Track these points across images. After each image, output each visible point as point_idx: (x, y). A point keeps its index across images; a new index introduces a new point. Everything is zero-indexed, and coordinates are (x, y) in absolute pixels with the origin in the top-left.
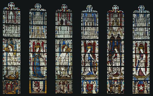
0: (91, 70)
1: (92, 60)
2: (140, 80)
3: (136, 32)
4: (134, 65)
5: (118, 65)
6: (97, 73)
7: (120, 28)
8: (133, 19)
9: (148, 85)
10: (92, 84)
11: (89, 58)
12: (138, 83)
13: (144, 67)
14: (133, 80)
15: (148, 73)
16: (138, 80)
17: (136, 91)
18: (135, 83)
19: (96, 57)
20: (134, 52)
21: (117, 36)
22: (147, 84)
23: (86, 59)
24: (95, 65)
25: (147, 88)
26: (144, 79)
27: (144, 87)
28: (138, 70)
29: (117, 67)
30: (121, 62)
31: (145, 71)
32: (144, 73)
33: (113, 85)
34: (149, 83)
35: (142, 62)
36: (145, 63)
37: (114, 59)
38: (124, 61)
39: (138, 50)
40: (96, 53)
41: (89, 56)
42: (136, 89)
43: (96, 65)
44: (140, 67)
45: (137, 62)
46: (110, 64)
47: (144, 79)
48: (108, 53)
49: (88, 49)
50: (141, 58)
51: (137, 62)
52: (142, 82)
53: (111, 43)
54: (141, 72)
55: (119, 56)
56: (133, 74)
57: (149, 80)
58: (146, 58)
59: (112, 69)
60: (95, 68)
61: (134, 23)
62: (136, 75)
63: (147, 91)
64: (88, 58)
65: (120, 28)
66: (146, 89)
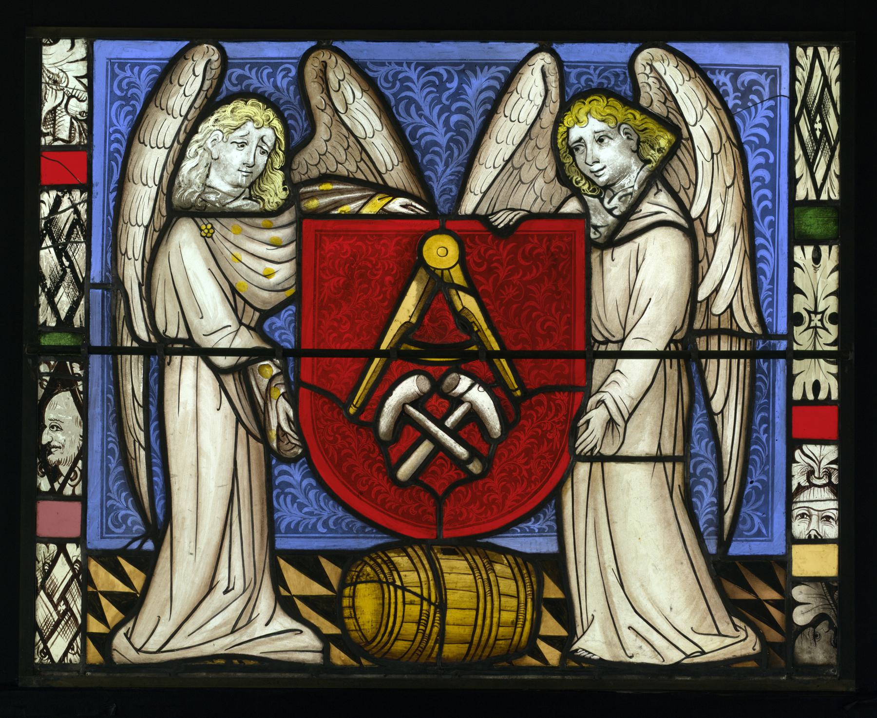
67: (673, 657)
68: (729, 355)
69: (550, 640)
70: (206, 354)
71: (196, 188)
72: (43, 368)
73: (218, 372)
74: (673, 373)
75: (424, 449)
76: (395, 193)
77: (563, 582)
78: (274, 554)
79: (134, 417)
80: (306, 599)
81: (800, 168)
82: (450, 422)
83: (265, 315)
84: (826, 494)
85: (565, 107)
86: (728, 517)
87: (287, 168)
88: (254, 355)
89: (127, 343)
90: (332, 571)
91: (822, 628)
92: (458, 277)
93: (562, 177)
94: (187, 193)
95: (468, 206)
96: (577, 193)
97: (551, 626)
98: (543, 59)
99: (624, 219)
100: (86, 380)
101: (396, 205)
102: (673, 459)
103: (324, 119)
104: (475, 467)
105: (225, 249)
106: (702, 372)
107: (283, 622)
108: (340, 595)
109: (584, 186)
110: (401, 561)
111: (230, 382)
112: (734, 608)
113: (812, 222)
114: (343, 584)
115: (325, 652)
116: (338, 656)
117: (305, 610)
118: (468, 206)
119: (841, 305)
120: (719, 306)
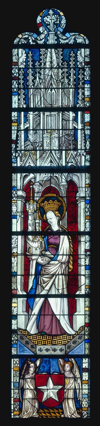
2: (45, 353)
4: (18, 285)
9: (81, 377)
12: (36, 367)
13: (61, 296)
14: (14, 352)
15: (80, 320)
16: (38, 353)
18: (21, 370)
20: (17, 226)
22: (77, 374)
26: (61, 350)
27: (63, 388)
28: (36, 310)
31: (66, 312)
32: (64, 322)
34: (85, 370)
35: (54, 268)
39: (38, 215)
42: (29, 395)
44: (44, 292)
45: (33, 271)
47: (61, 350)
50: (48, 253)
51: (33, 271)
52: (53, 362)
54: (48, 319)
56: (14, 327)
57: (85, 356)
58: (74, 255)
62: (24, 333)
63: (79, 407)
66: (71, 394)
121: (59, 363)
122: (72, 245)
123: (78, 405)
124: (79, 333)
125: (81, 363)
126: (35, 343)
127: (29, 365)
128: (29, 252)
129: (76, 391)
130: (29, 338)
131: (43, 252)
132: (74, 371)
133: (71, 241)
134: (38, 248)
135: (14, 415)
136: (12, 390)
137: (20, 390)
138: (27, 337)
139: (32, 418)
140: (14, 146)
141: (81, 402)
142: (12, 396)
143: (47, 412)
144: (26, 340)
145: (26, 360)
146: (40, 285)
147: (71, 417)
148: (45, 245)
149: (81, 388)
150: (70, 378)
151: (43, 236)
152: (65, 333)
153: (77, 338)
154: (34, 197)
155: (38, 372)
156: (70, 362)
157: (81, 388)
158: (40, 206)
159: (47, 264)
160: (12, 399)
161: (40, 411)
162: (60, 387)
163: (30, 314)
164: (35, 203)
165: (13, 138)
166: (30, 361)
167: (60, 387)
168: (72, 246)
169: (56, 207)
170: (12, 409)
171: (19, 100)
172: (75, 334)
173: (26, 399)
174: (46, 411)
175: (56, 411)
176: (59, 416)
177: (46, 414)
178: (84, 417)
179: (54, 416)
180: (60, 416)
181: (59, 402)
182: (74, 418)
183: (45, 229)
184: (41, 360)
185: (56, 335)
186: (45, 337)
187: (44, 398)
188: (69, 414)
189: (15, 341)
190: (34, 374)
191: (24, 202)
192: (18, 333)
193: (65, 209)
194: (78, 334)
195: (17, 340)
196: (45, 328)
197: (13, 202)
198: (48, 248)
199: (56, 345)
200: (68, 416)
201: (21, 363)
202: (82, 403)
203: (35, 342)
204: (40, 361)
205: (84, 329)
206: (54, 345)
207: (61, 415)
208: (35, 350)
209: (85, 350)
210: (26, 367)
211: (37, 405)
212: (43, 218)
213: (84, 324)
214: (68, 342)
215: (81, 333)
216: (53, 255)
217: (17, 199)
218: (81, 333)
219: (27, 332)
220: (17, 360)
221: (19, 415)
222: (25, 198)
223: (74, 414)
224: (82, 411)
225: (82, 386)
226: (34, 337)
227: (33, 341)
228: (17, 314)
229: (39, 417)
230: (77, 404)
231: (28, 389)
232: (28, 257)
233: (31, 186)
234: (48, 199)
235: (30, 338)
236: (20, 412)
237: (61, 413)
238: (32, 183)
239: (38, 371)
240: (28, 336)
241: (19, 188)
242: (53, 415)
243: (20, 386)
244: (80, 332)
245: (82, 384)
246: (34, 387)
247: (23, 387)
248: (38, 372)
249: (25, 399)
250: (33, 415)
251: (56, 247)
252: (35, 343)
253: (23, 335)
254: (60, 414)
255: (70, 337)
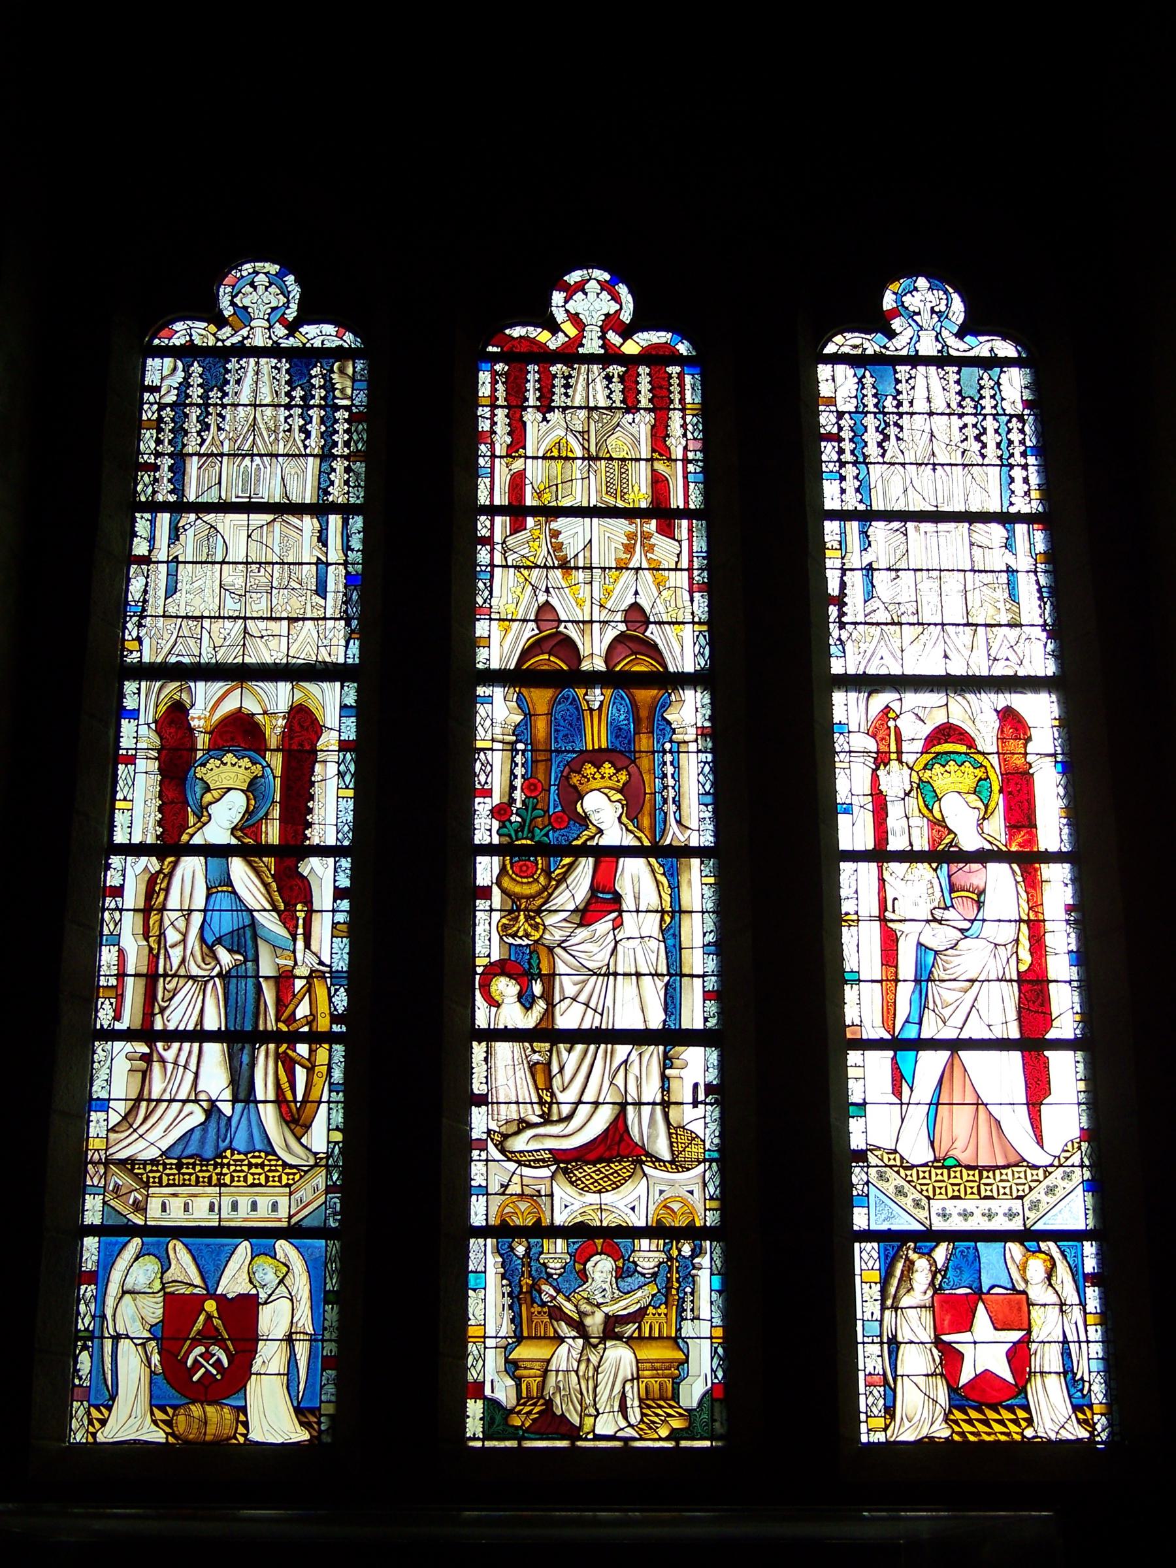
0: (234, 1082)
1: (264, 951)
2: (957, 1224)
3: (869, 569)
5: (627, 1019)
6: (319, 1137)
7: (646, 536)
8: (827, 421)
9: (1083, 1304)
10: (243, 1287)
11: (225, 923)
16: (939, 1225)
17: (910, 1398)
19: (323, 897)
21: (611, 634)
22: (1070, 1293)
23: (172, 936)
24: (303, 1010)
25: (1066, 1354)
27: (1026, 1341)
29: (622, 1051)
30: (675, 976)
33: (557, 1314)
36: (1022, 980)
37: (583, 933)
38: (712, 964)
40: (322, 851)
41: (221, 884)
43: (312, 1019)
45: (907, 967)
46: (526, 1000)
47: (1011, 1215)
48: (489, 850)
49: (208, 789)
51: (907, 967)
53: (529, 715)
55: (650, 898)
56: (857, 1142)
59: (542, 1075)
60: (289, 1065)
61: (842, 464)
64: (197, 918)
65: (646, 536)
67: (280, 1441)
68: (303, 1340)
69: (241, 1435)
70: (132, 1339)
71: (132, 1284)
72: (79, 1343)
73: (136, 1345)
74: (284, 1346)
75: (203, 1370)
76: (196, 1286)
77: (246, 1415)
78: (151, 1406)
79: (108, 1360)
80: (162, 1421)
81: (328, 1280)
82: (211, 1362)
83: (152, 1326)
84: (333, 1386)
85: (252, 1259)
86: (301, 1394)
87: (161, 1278)
88: (149, 1339)
89: (107, 1335)
90: (170, 1411)
91: (330, 1431)
92: (216, 1315)
93: (251, 1282)
94: (128, 1287)
95: (219, 1292)
96: (255, 1287)
97: (241, 1429)
98: (246, 1243)
99: (270, 1296)
100: (92, 1347)
101: (196, 1291)
102: (284, 1374)
103: (173, 1262)
104: (219, 1377)
105: (140, 1305)
106: (294, 1346)
107: (154, 1428)
108: (172, 1419)
109: (257, 1284)
110: (193, 1408)
111: (139, 1348)
112: (302, 1424)
113: (331, 1297)
114: (174, 1415)
115: (167, 1438)
116: (171, 1440)
117: (160, 1424)
118: (219, 1292)
119: (339, 1324)
120: (300, 1324)
121: (1008, 1256)
122: (1026, 891)
123: (1079, 1394)
124: (1062, 1160)
125: (1080, 1257)
126: (925, 1193)
127: (913, 1263)
128: (894, 911)
129: (1069, 1348)
130: (906, 1176)
131: (938, 914)
132: (1059, 1281)
133: (1020, 879)
134: (921, 902)
135: (869, 1430)
136: (860, 1347)
137: (886, 1346)
138: (898, 1173)
139: (927, 1445)
140: (833, 611)
141: (1087, 1385)
142: (861, 1366)
143: (978, 1420)
144: (896, 1183)
145: (900, 1248)
146: (934, 1011)
147: (1059, 1436)
148: (942, 891)
149: (1083, 1338)
150: (1045, 1305)
151: (934, 865)
152: (1021, 1161)
153: (1059, 1178)
154: (899, 752)
155: (941, 1288)
156: (1044, 1253)
157: (1083, 1338)
158: (920, 779)
159: (952, 948)
160: (861, 1375)
161: (952, 1417)
162: (1016, 1335)
163: (905, 1099)
164: (906, 771)
165: (830, 591)
166: (915, 1251)
167: (1016, 1335)
168: (1024, 895)
169: (969, 782)
170: (863, 1408)
171: (843, 491)
172: (1051, 1165)
173: (908, 1376)
174: (974, 1414)
175: (1007, 1415)
176: (1017, 1433)
177: (974, 1426)
178: (1099, 1435)
179: (1002, 1433)
180: (1022, 1434)
181: (1016, 1385)
182: (1068, 1441)
183: (940, 844)
184: (951, 1246)
185: (994, 1168)
186: (955, 1172)
187: (966, 1376)
188: (1049, 1425)
189: (860, 1187)
190: (930, 1293)
191: (874, 767)
192: (870, 1160)
193: (996, 787)
194: (1061, 1165)
195: (867, 1183)
196: (954, 1146)
197: (837, 765)
198: (952, 899)
199: (992, 1198)
200: (1048, 1431)
201: (886, 1257)
202: (1090, 1390)
203: (925, 1188)
204: (947, 1249)
205: (1079, 1148)
206: (986, 1198)
207: (1023, 1430)
208: (927, 1215)
209: (1086, 1214)
210: (902, 1271)
211: (942, 1395)
212: (931, 811)
213: (1077, 1134)
214: (1031, 1189)
215: (1069, 1162)
216: (969, 920)
217: (852, 759)
218: (1069, 1162)
219: (897, 1156)
220: (871, 1247)
221: (885, 1429)
222: (875, 755)
223: (1066, 1426)
224: (1093, 1414)
225: (1086, 1331)
226: (921, 1175)
227: (918, 1187)
228: (864, 1099)
229: (951, 1435)
230: (1073, 1391)
231: (912, 1342)
232: (890, 924)
233: (891, 724)
234: (941, 759)
235: (909, 1178)
236: (888, 1422)
237: (1024, 1424)
238: (892, 715)
239: (940, 1285)
240: (901, 1170)
241: (853, 727)
242: (997, 1428)
243: (885, 1334)
244: (1067, 1159)
245: (1086, 1326)
246: (932, 1336)
247: (895, 1337)
248: (941, 1288)
249: (902, 1376)
250: (931, 1431)
251: (975, 897)
252: (925, 1193)
253: (886, 1166)
254: (1019, 1426)
255: (1035, 1172)
